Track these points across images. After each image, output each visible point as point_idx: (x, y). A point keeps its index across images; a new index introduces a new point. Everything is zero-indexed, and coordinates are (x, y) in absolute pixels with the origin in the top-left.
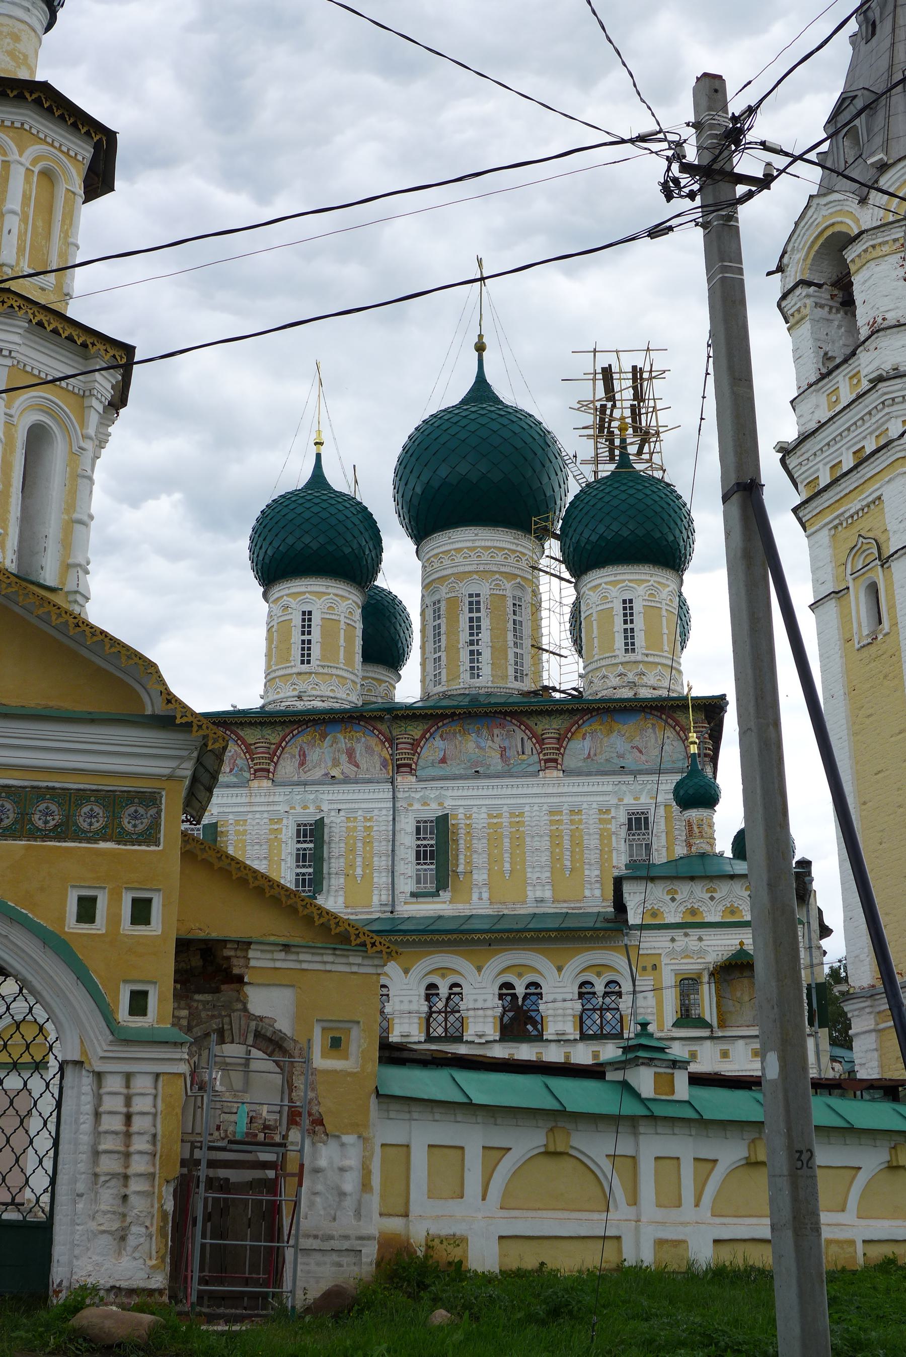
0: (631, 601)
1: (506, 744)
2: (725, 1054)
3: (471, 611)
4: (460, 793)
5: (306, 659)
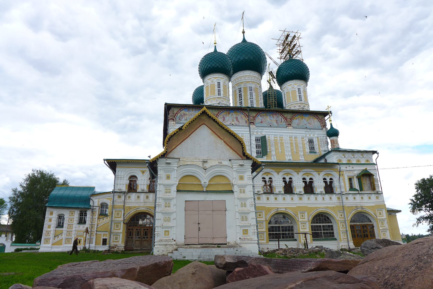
1: (277, 119)
2: (362, 198)
4: (267, 131)
5: (219, 94)
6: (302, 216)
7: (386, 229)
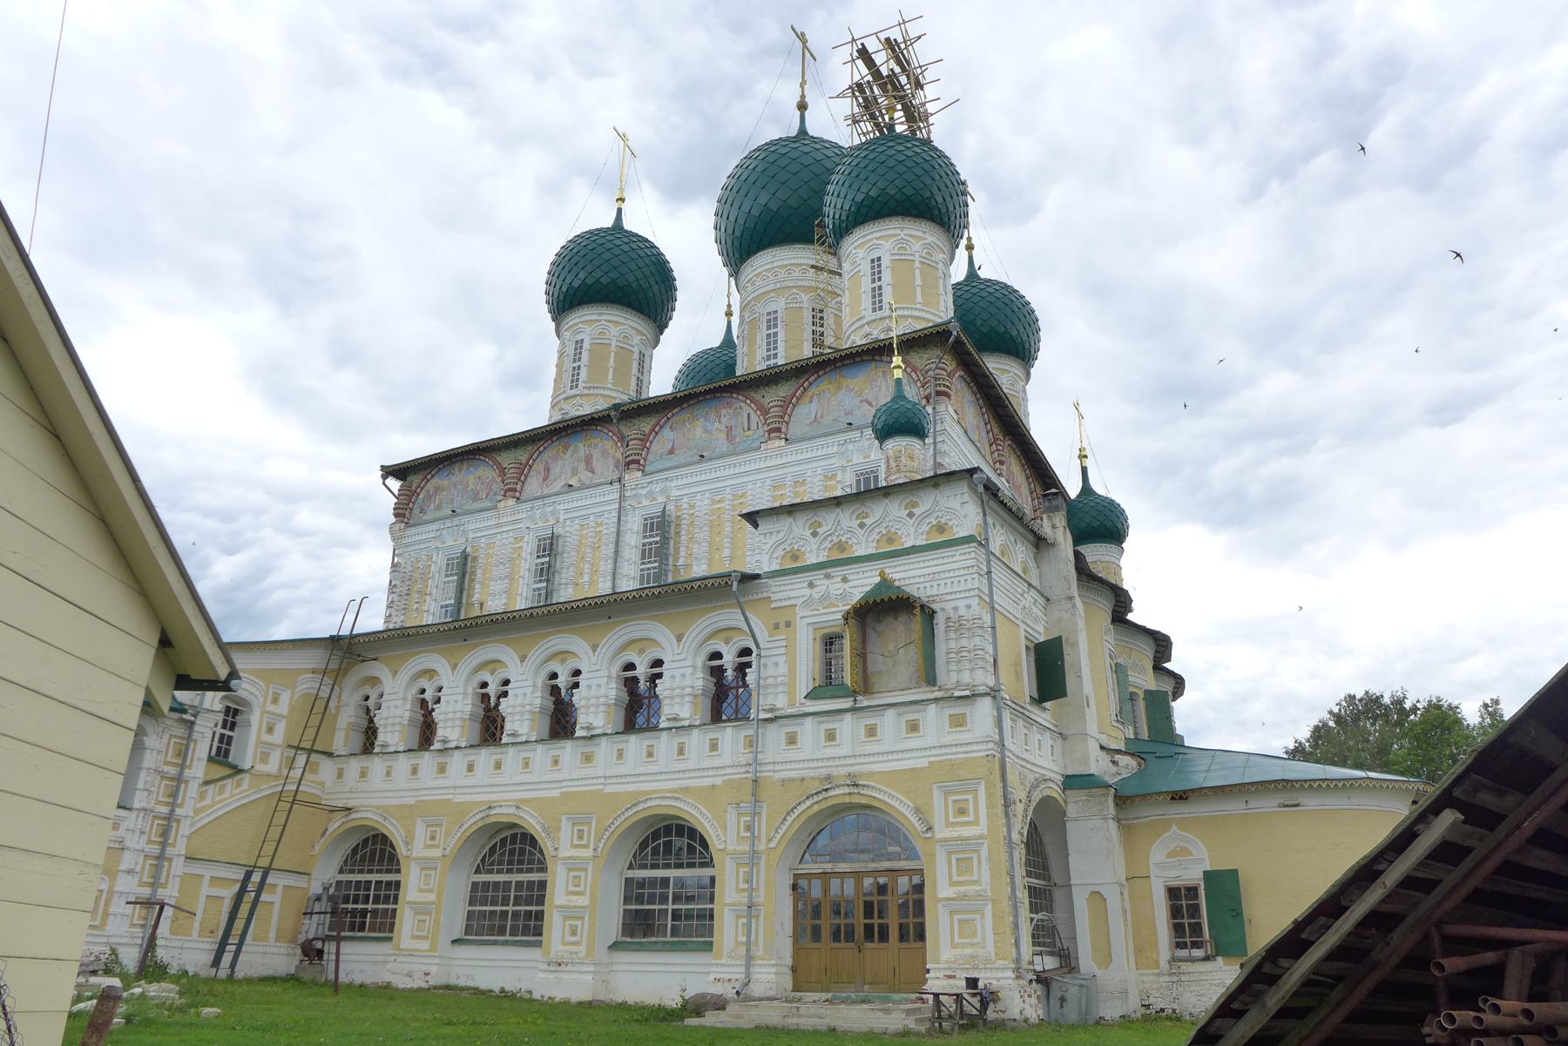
0: (879, 259)
1: (733, 423)
2: (871, 731)
3: (769, 328)
6: (580, 837)
7: (979, 896)
